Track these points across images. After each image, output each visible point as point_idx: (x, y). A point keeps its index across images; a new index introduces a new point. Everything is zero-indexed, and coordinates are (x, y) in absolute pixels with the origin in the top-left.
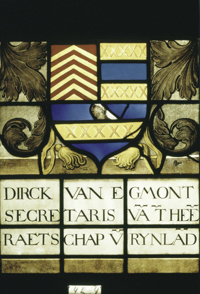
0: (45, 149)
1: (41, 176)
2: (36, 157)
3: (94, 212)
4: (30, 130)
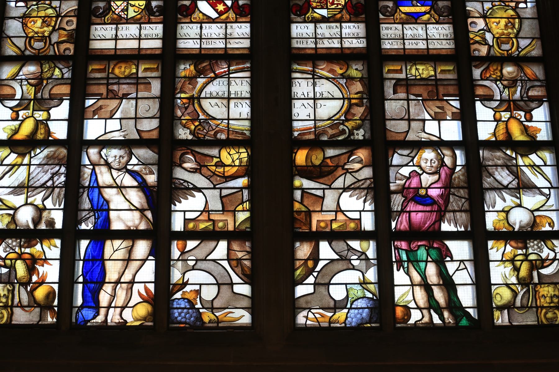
0: (396, 15)
1: (395, 23)
2: (393, 17)
3: (415, 35)
4: (390, 8)
